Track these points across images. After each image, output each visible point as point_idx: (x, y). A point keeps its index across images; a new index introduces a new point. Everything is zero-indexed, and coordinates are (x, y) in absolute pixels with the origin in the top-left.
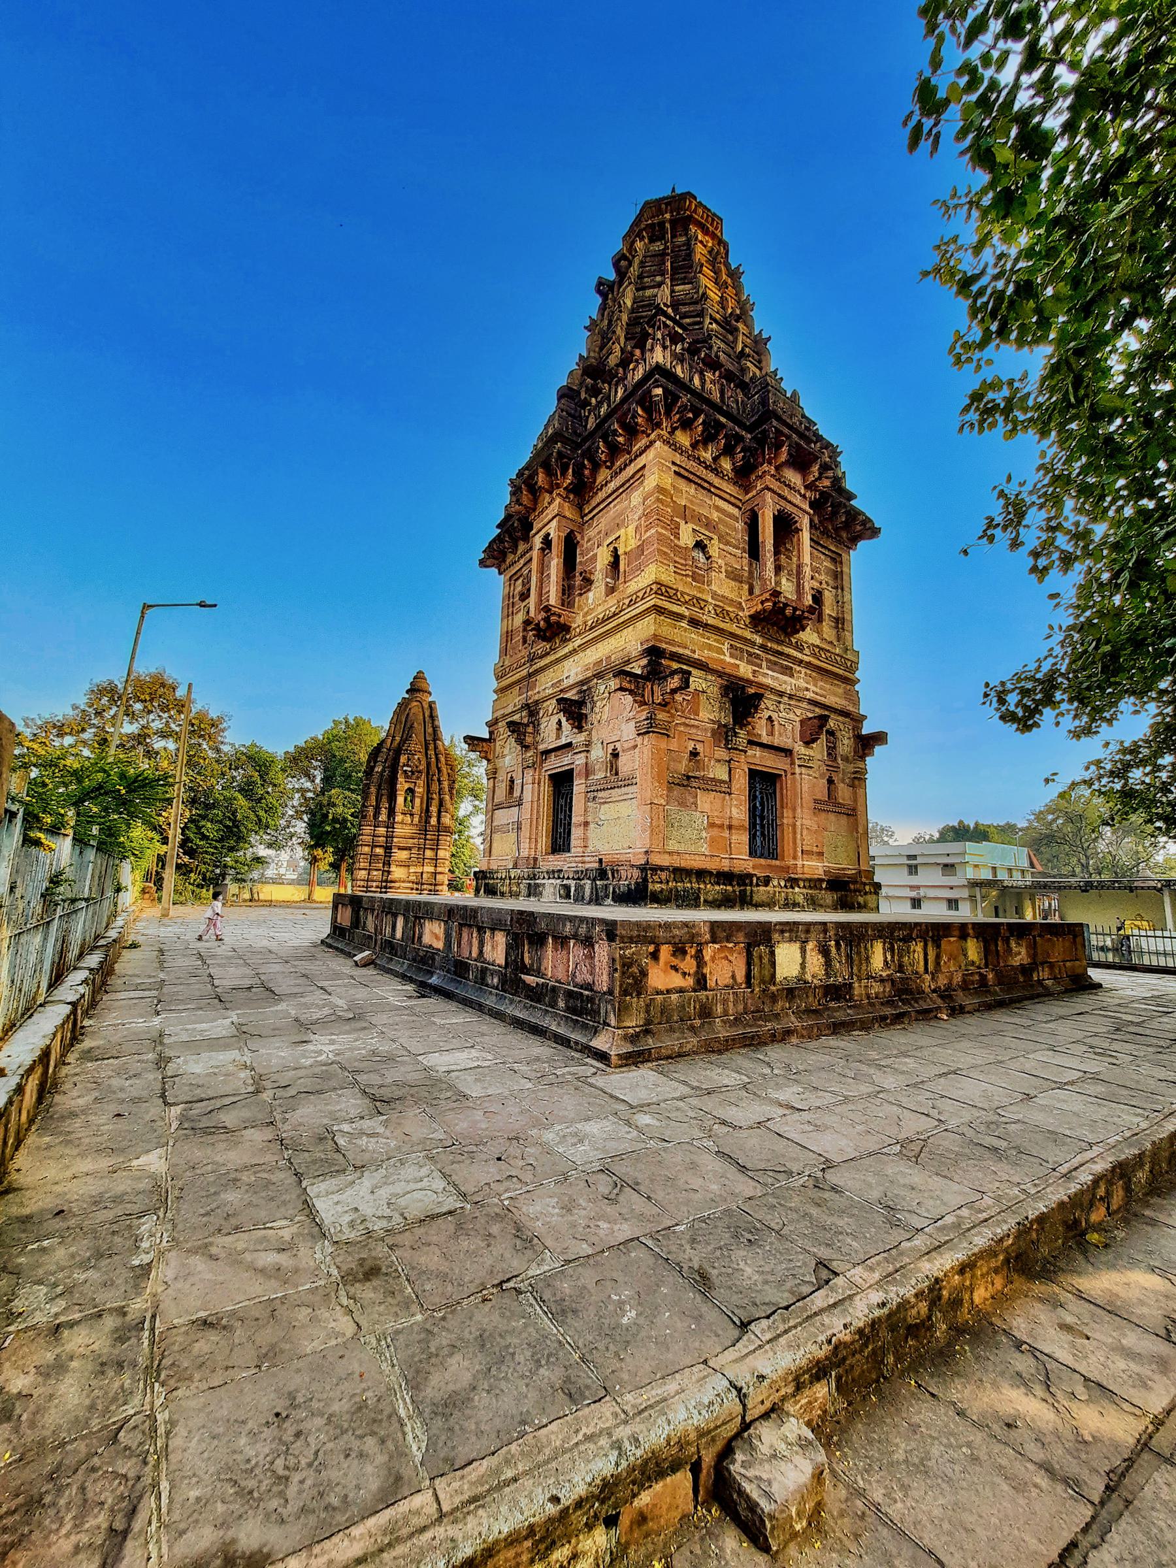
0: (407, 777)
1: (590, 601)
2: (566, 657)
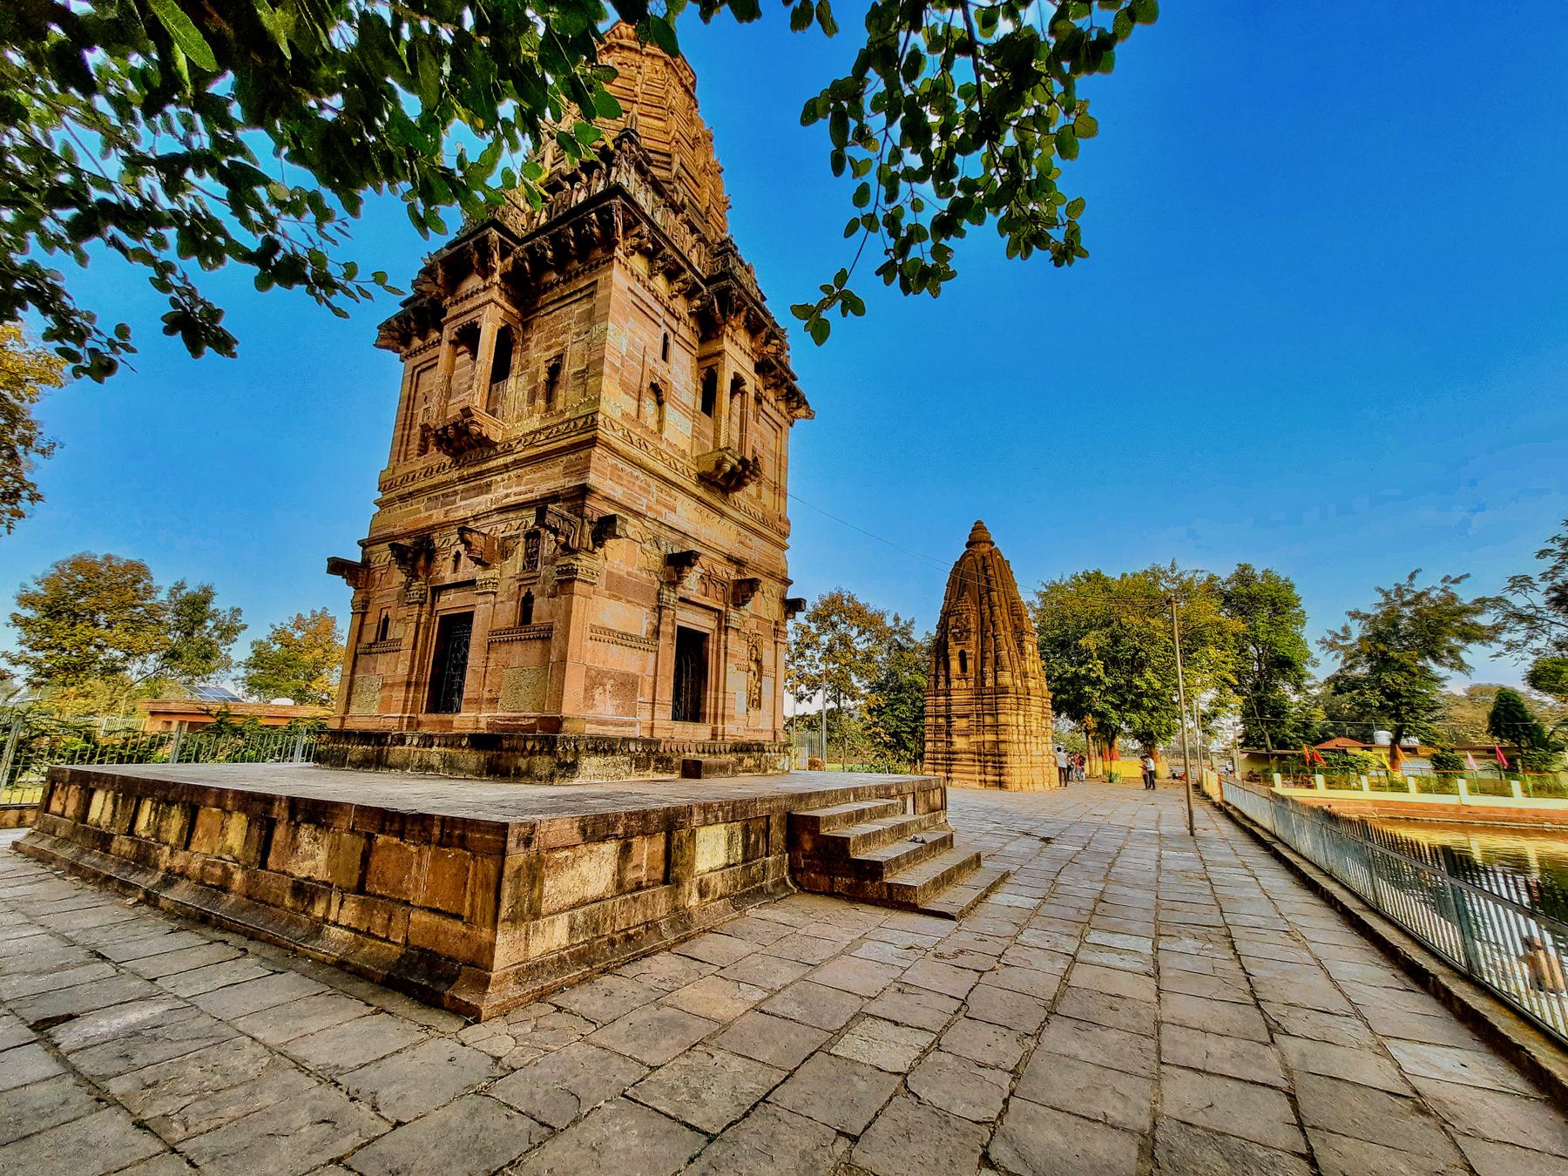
0: (956, 639)
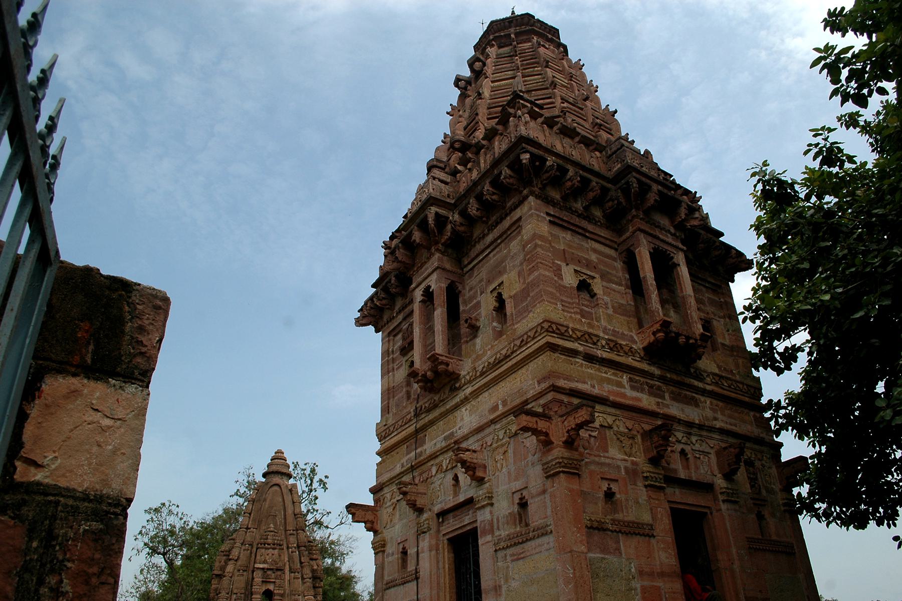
1: (478, 347)
2: (457, 407)
